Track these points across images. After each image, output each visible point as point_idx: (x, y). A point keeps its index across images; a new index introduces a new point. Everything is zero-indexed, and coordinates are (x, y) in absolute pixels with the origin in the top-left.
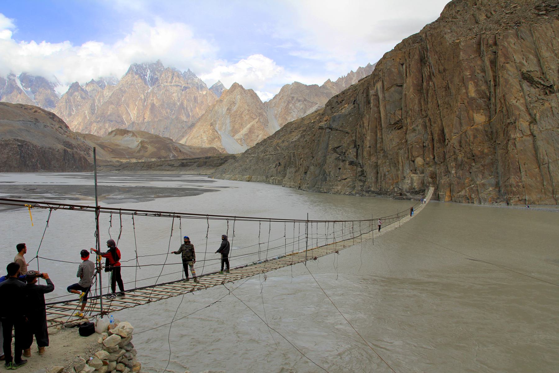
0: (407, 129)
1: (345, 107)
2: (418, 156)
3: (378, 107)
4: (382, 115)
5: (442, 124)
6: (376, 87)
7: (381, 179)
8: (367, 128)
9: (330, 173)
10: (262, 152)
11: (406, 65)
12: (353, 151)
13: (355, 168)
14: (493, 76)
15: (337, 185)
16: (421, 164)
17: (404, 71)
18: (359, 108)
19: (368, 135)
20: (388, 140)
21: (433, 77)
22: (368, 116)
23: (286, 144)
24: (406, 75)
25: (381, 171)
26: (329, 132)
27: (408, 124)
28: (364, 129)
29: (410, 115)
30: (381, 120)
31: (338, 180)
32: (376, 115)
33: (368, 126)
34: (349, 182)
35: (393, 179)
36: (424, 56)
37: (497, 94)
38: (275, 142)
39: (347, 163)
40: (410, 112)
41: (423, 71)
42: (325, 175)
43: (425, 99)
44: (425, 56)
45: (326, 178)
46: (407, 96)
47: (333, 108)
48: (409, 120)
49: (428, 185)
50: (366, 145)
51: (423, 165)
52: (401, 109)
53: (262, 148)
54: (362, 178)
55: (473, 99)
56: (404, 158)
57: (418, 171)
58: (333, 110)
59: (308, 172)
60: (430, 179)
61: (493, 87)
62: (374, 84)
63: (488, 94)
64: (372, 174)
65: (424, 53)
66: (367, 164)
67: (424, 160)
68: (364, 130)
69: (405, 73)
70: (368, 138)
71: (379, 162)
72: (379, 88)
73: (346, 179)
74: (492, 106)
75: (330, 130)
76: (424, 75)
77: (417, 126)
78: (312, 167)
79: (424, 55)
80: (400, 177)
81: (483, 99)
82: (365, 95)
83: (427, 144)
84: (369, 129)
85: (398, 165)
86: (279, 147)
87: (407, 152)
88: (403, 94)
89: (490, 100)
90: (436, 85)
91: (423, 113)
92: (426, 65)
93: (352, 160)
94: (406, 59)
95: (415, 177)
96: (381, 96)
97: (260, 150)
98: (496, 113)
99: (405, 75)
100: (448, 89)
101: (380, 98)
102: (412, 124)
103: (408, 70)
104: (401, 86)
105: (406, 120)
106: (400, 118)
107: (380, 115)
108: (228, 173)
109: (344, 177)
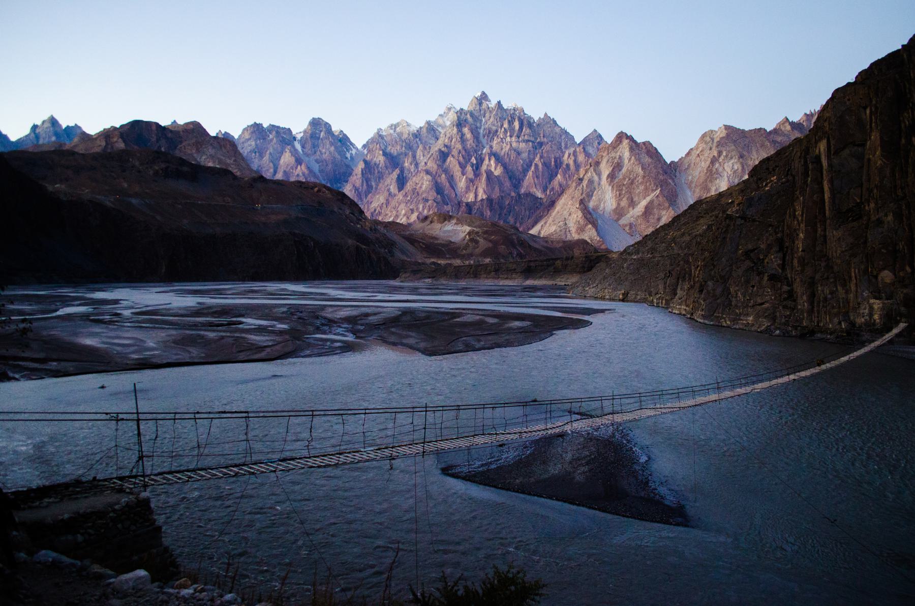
0: (869, 219)
1: (772, 181)
2: (884, 269)
4: (827, 196)
8: (800, 219)
9: (737, 294)
10: (648, 252)
11: (871, 110)
12: (777, 257)
13: (779, 286)
15: (748, 315)
16: (888, 281)
19: (801, 231)
20: (835, 239)
22: (801, 198)
23: (687, 238)
25: (819, 292)
26: (741, 224)
28: (795, 220)
31: (750, 305)
34: (767, 309)
35: (839, 307)
38: (671, 234)
39: (766, 278)
40: (875, 191)
41: (901, 118)
42: (730, 296)
44: (907, 91)
45: (731, 301)
47: (760, 179)
48: (872, 205)
49: (898, 318)
50: (798, 248)
51: (893, 284)
52: (861, 185)
53: (650, 244)
54: (790, 303)
56: (859, 270)
57: (883, 295)
58: (759, 182)
59: (705, 291)
60: (902, 309)
62: (816, 143)
64: (805, 298)
66: (798, 280)
67: (895, 274)
69: (869, 124)
70: (801, 235)
71: (817, 277)
72: (822, 149)
73: (762, 304)
75: (743, 221)
76: (903, 126)
77: (886, 215)
78: (710, 283)
80: (851, 305)
82: (802, 160)
83: (901, 247)
84: (802, 220)
86: (675, 244)
87: (864, 260)
88: (866, 160)
91: (900, 193)
93: (773, 272)
94: (871, 99)
95: (877, 304)
96: (825, 163)
99: (868, 127)
101: (824, 165)
102: (878, 212)
103: (873, 117)
104: (863, 145)
105: (869, 205)
106: (858, 201)
107: (824, 196)
108: (594, 285)
109: (759, 301)
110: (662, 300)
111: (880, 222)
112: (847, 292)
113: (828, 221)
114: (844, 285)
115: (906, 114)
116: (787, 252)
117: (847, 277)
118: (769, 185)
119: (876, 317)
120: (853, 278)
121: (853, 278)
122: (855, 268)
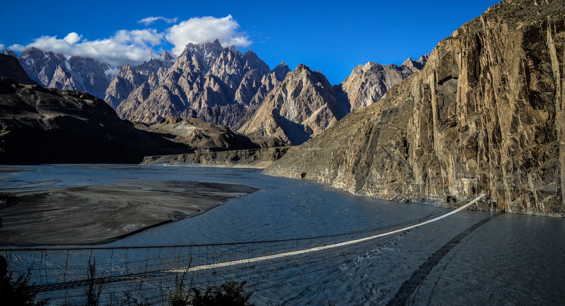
3: (430, 102)
5: (497, 121)
6: (428, 79)
7: (429, 183)
8: (417, 125)
11: (462, 54)
14: (560, 66)
17: (460, 61)
18: (413, 101)
21: (490, 68)
24: (462, 66)
27: (462, 121)
28: (414, 125)
29: (464, 111)
30: (432, 117)
32: (427, 110)
33: (418, 123)
35: (442, 184)
36: (483, 44)
37: (563, 87)
41: (481, 61)
43: (481, 93)
46: (462, 90)
55: (533, 92)
61: (559, 79)
63: (554, 87)
64: (420, 177)
65: (483, 40)
68: (414, 127)
69: (460, 64)
72: (431, 80)
74: (557, 101)
76: (482, 66)
79: (483, 43)
81: (548, 93)
84: (418, 126)
85: (449, 167)
88: (458, 88)
89: (555, 94)
90: (493, 77)
92: (485, 54)
95: (466, 181)
97: (318, 144)
98: (561, 109)
99: (460, 66)
100: (506, 81)
103: (463, 60)
105: (460, 116)
106: (454, 114)
110: (328, 179)
111: (467, 128)
112: (447, 174)
113: (435, 127)
114: (445, 169)
115: (483, 58)
116: (409, 146)
117: (447, 164)
118: (398, 103)
119: (466, 190)
120: (451, 164)
121: (451, 164)
122: (452, 158)
